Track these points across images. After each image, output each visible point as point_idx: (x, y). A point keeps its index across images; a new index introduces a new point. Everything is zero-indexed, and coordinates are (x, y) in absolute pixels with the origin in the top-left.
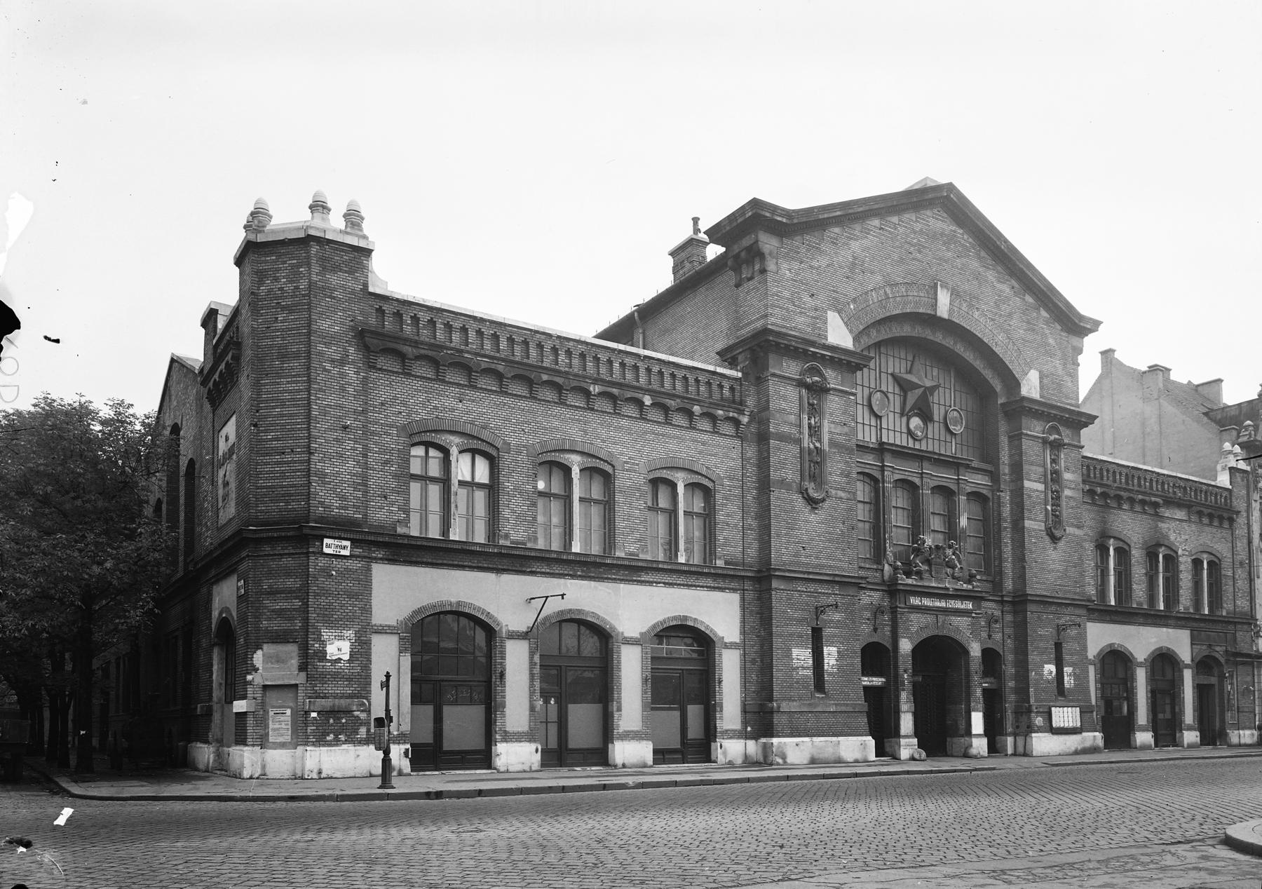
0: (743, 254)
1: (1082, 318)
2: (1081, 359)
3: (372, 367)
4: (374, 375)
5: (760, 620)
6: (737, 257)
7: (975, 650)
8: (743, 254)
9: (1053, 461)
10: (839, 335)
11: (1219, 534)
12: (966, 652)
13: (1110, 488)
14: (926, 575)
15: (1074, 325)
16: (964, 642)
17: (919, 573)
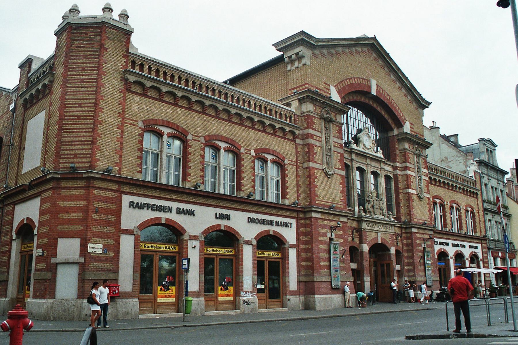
0: (294, 57)
1: (424, 100)
2: (424, 118)
3: (129, 90)
4: (129, 95)
5: (306, 234)
6: (290, 57)
7: (393, 250)
8: (294, 57)
9: (418, 163)
10: (336, 97)
11: (473, 199)
12: (389, 250)
13: (439, 177)
14: (372, 214)
15: (422, 104)
16: (389, 246)
17: (370, 212)
